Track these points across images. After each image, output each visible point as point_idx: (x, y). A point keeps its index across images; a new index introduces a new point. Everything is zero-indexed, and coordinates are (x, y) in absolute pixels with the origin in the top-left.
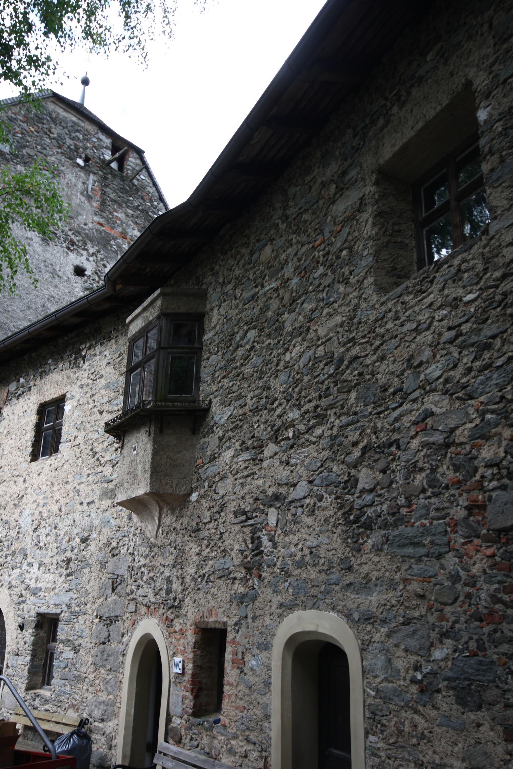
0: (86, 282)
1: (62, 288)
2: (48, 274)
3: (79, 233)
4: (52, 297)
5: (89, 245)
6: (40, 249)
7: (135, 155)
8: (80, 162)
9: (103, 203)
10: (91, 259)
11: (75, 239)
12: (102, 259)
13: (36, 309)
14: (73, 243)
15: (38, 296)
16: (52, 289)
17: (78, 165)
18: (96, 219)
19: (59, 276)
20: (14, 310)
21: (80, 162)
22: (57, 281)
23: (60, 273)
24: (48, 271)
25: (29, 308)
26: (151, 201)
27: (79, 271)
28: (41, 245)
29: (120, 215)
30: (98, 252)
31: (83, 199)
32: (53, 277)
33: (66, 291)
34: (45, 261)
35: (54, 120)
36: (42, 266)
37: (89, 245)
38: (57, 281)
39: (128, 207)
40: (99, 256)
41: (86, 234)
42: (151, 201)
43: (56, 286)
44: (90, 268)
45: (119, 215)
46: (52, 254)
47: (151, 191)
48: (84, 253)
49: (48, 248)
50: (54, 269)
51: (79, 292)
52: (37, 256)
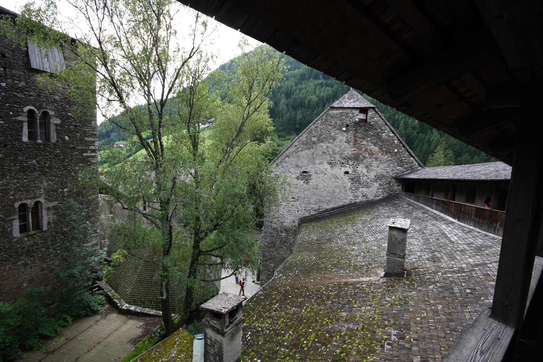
3: (345, 159)
5: (350, 161)
6: (330, 171)
7: (371, 110)
8: (344, 129)
9: (356, 141)
11: (343, 161)
14: (343, 163)
17: (344, 131)
18: (352, 149)
21: (344, 129)
22: (337, 180)
26: (380, 128)
27: (347, 173)
29: (364, 142)
31: (346, 144)
35: (332, 117)
37: (350, 161)
38: (337, 180)
39: (368, 137)
40: (355, 164)
41: (348, 158)
42: (380, 128)
44: (350, 171)
45: (364, 143)
47: (381, 123)
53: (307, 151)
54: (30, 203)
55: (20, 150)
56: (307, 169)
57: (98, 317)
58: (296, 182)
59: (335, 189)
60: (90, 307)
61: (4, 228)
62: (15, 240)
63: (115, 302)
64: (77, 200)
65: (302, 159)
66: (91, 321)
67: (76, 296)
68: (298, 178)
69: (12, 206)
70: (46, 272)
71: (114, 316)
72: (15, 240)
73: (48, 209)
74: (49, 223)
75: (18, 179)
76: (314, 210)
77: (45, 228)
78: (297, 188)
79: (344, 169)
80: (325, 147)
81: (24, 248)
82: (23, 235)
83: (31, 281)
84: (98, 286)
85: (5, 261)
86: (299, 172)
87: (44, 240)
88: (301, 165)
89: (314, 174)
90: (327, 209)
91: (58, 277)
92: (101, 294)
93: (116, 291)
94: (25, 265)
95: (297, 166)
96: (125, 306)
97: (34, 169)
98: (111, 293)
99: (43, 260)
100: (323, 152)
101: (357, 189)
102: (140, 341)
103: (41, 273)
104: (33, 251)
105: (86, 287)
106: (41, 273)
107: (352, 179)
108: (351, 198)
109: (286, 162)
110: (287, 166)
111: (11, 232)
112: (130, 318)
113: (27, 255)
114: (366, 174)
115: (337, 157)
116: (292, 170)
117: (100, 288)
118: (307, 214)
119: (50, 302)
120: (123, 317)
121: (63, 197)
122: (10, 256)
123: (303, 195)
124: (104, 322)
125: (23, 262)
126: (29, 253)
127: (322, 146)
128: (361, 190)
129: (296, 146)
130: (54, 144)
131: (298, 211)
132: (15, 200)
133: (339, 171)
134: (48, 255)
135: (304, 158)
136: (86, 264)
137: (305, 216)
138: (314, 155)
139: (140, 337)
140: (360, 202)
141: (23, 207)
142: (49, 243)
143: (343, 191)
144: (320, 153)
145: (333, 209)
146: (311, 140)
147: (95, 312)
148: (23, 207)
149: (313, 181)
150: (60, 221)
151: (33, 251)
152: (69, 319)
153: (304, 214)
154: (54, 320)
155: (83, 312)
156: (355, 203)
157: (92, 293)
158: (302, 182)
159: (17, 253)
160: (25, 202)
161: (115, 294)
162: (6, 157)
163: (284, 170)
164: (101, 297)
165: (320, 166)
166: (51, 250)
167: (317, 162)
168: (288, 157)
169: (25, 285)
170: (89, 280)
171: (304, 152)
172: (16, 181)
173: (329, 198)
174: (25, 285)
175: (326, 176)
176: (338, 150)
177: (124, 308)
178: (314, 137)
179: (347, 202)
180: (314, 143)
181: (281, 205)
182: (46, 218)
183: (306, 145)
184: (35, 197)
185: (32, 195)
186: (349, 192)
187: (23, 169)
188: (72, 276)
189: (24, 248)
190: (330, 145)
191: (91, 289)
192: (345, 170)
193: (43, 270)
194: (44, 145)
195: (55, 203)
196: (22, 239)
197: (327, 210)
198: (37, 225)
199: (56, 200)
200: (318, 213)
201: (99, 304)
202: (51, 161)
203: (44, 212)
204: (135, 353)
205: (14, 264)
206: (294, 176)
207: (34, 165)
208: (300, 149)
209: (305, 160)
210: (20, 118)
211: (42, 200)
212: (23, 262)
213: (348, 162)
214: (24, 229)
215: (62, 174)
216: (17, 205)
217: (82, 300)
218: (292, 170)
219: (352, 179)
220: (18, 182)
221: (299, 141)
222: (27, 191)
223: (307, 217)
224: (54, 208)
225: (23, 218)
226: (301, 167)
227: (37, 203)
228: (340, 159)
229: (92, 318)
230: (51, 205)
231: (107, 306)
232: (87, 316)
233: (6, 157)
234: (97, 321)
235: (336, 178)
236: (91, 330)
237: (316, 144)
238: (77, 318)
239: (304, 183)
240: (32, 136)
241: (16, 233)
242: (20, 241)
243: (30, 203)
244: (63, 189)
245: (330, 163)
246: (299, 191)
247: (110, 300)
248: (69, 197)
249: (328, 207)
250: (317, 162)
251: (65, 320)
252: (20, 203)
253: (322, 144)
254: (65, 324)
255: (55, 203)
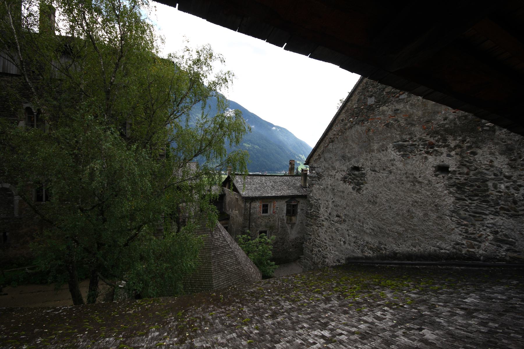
0: (451, 178)
1: (424, 192)
2: (410, 184)
3: (437, 133)
4: (416, 202)
5: (450, 139)
6: (400, 165)
10: (453, 153)
11: (432, 140)
12: (469, 148)
13: (403, 214)
14: (431, 145)
15: (403, 204)
16: (414, 195)
19: (419, 183)
20: (387, 218)
22: (418, 186)
23: (420, 180)
24: (409, 181)
25: (398, 214)
27: (443, 169)
28: (401, 161)
30: (463, 141)
32: (414, 185)
33: (428, 193)
34: (406, 173)
36: (404, 178)
37: (450, 139)
38: (418, 186)
41: (446, 130)
43: (418, 192)
44: (452, 164)
46: (411, 165)
48: (444, 150)
49: (408, 161)
50: (415, 177)
51: (442, 192)
52: (399, 172)
53: (358, 127)
56: (358, 162)
58: (342, 186)
59: (413, 209)
65: (350, 142)
68: (344, 180)
76: (371, 249)
78: (342, 198)
79: (433, 161)
80: (390, 113)
86: (346, 169)
88: (349, 155)
89: (369, 172)
90: (395, 254)
95: (344, 157)
100: (387, 125)
101: (478, 215)
107: (460, 187)
108: (458, 238)
109: (329, 151)
110: (331, 158)
114: (507, 171)
115: (417, 130)
116: (337, 165)
118: (358, 254)
123: (352, 214)
127: (383, 113)
128: (490, 220)
129: (342, 120)
131: (345, 242)
133: (425, 165)
135: (353, 141)
137: (355, 255)
138: (371, 133)
140: (487, 258)
143: (433, 216)
144: (381, 127)
145: (409, 256)
146: (365, 104)
149: (368, 188)
153: (353, 251)
156: (472, 257)
158: (350, 187)
163: (327, 165)
165: (380, 155)
167: (376, 147)
168: (332, 142)
171: (353, 130)
173: (401, 229)
175: (392, 177)
176: (420, 113)
178: (371, 96)
179: (447, 247)
180: (371, 108)
181: (323, 225)
183: (357, 115)
186: (450, 223)
190: (400, 106)
192: (437, 163)
197: (394, 256)
200: (378, 258)
206: (339, 176)
208: (349, 125)
209: (354, 146)
213: (445, 140)
218: (337, 165)
219: (460, 187)
221: (347, 111)
223: (357, 258)
226: (349, 159)
228: (424, 136)
235: (415, 181)
237: (373, 110)
239: (353, 189)
245: (399, 148)
246: (347, 205)
249: (395, 248)
250: (376, 147)
253: (385, 108)
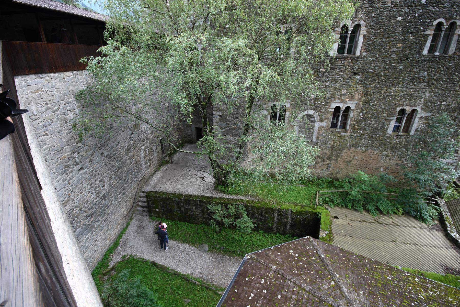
54: (409, 109)
55: (417, 62)
57: (424, 225)
60: (421, 213)
61: (384, 124)
62: (387, 135)
63: (446, 224)
64: (451, 116)
66: (417, 224)
67: (414, 197)
69: (395, 109)
70: (399, 167)
71: (439, 235)
72: (387, 135)
73: (421, 117)
74: (417, 130)
75: (407, 88)
77: (412, 133)
81: (391, 143)
82: (394, 133)
83: (387, 169)
84: (436, 201)
85: (376, 147)
87: (408, 142)
91: (406, 175)
92: (436, 209)
93: (452, 216)
94: (387, 156)
96: (454, 234)
97: (423, 80)
98: (446, 214)
99: (401, 158)
102: (453, 274)
103: (395, 167)
104: (396, 148)
105: (425, 195)
106: (395, 167)
111: (387, 129)
112: (454, 249)
113: (391, 149)
117: (437, 204)
119: (393, 190)
120: (448, 243)
121: (439, 110)
122: (380, 146)
124: (427, 232)
125: (386, 153)
126: (393, 149)
130: (450, 56)
132: (399, 105)
134: (406, 156)
136: (434, 176)
139: (456, 271)
141: (403, 111)
142: (411, 147)
147: (423, 220)
148: (403, 111)
150: (427, 131)
151: (396, 148)
152: (401, 211)
154: (390, 204)
155: (414, 213)
157: (428, 203)
159: (385, 145)
160: (405, 108)
161: (449, 217)
162: (405, 68)
164: (434, 211)
166: (409, 153)
169: (382, 169)
170: (431, 191)
172: (405, 89)
174: (382, 169)
177: (452, 234)
182: (416, 124)
184: (414, 106)
185: (413, 104)
187: (413, 80)
188: (417, 180)
189: (391, 143)
191: (429, 200)
193: (397, 165)
194: (440, 57)
195: (428, 114)
196: (392, 136)
198: (407, 129)
199: (431, 111)
201: (430, 216)
202: (440, 74)
203: (417, 120)
204: (443, 279)
205: (381, 152)
207: (424, 77)
210: (428, 32)
211: (419, 109)
212: (386, 153)
214: (396, 129)
215: (446, 88)
216: (398, 109)
217: (416, 203)
220: (406, 91)
222: (410, 99)
224: (427, 118)
225: (399, 120)
227: (414, 111)
229: (418, 222)
230: (424, 114)
231: (436, 222)
232: (415, 217)
233: (405, 68)
234: (422, 228)
236: (413, 231)
238: (407, 213)
240: (432, 49)
241: (390, 131)
242: (390, 137)
243: (409, 109)
244: (441, 102)
247: (441, 219)
248: (444, 110)
251: (397, 209)
252: (401, 108)
254: (397, 212)
255: (428, 114)
